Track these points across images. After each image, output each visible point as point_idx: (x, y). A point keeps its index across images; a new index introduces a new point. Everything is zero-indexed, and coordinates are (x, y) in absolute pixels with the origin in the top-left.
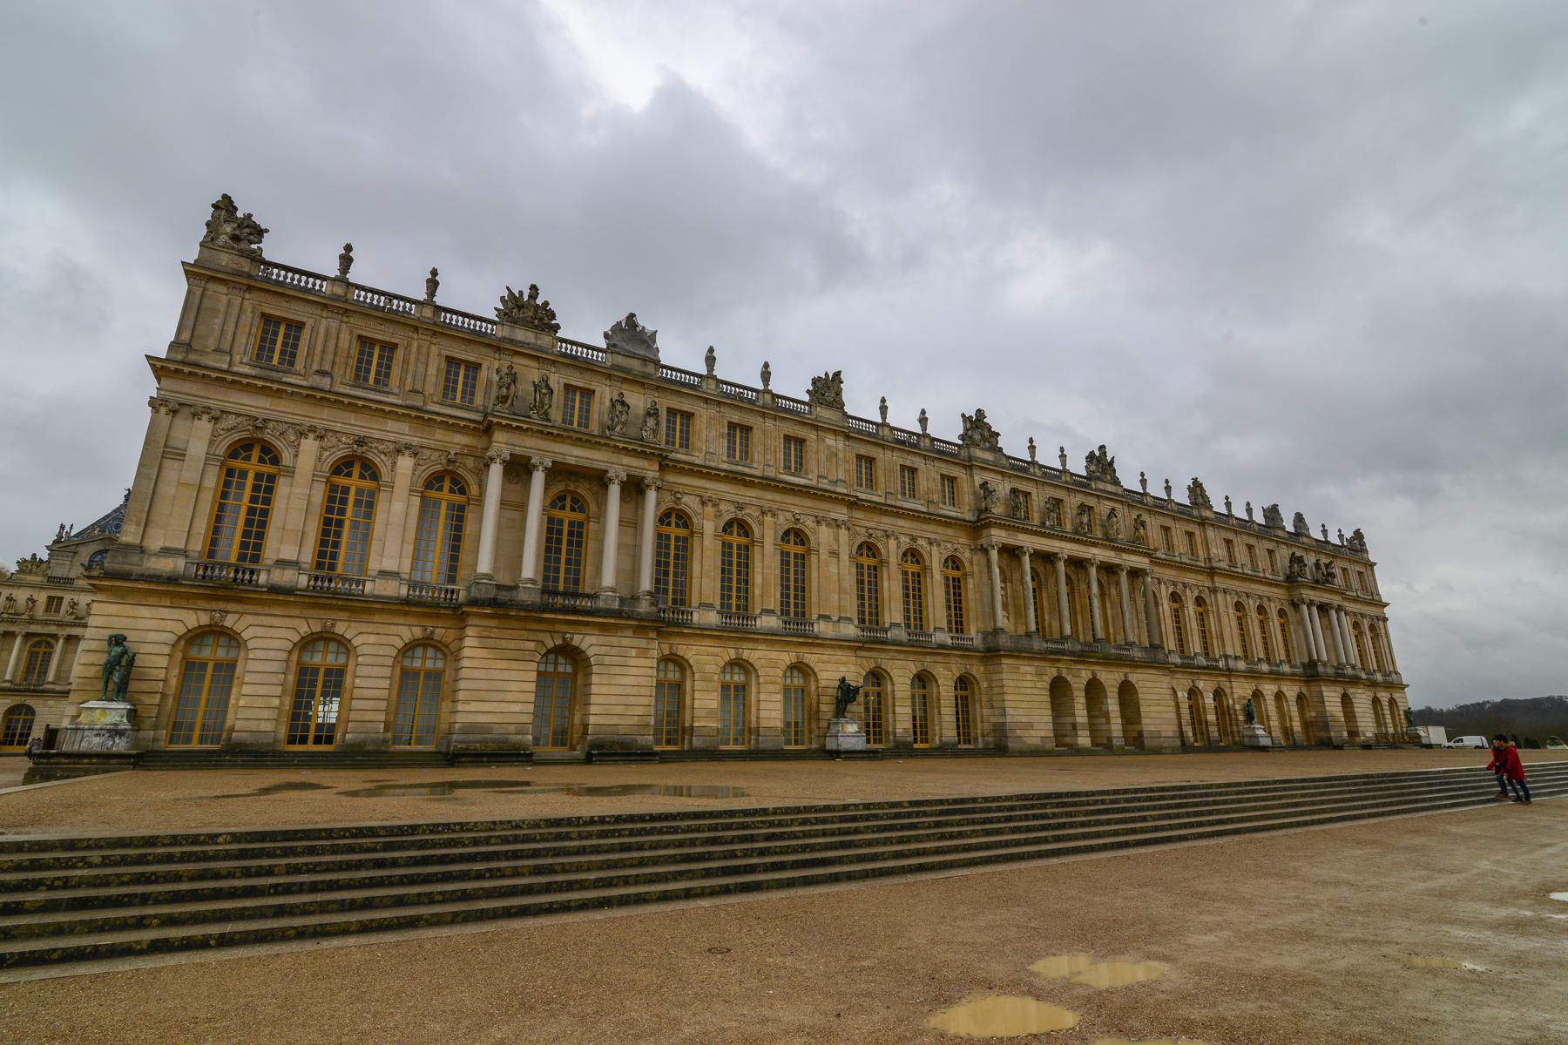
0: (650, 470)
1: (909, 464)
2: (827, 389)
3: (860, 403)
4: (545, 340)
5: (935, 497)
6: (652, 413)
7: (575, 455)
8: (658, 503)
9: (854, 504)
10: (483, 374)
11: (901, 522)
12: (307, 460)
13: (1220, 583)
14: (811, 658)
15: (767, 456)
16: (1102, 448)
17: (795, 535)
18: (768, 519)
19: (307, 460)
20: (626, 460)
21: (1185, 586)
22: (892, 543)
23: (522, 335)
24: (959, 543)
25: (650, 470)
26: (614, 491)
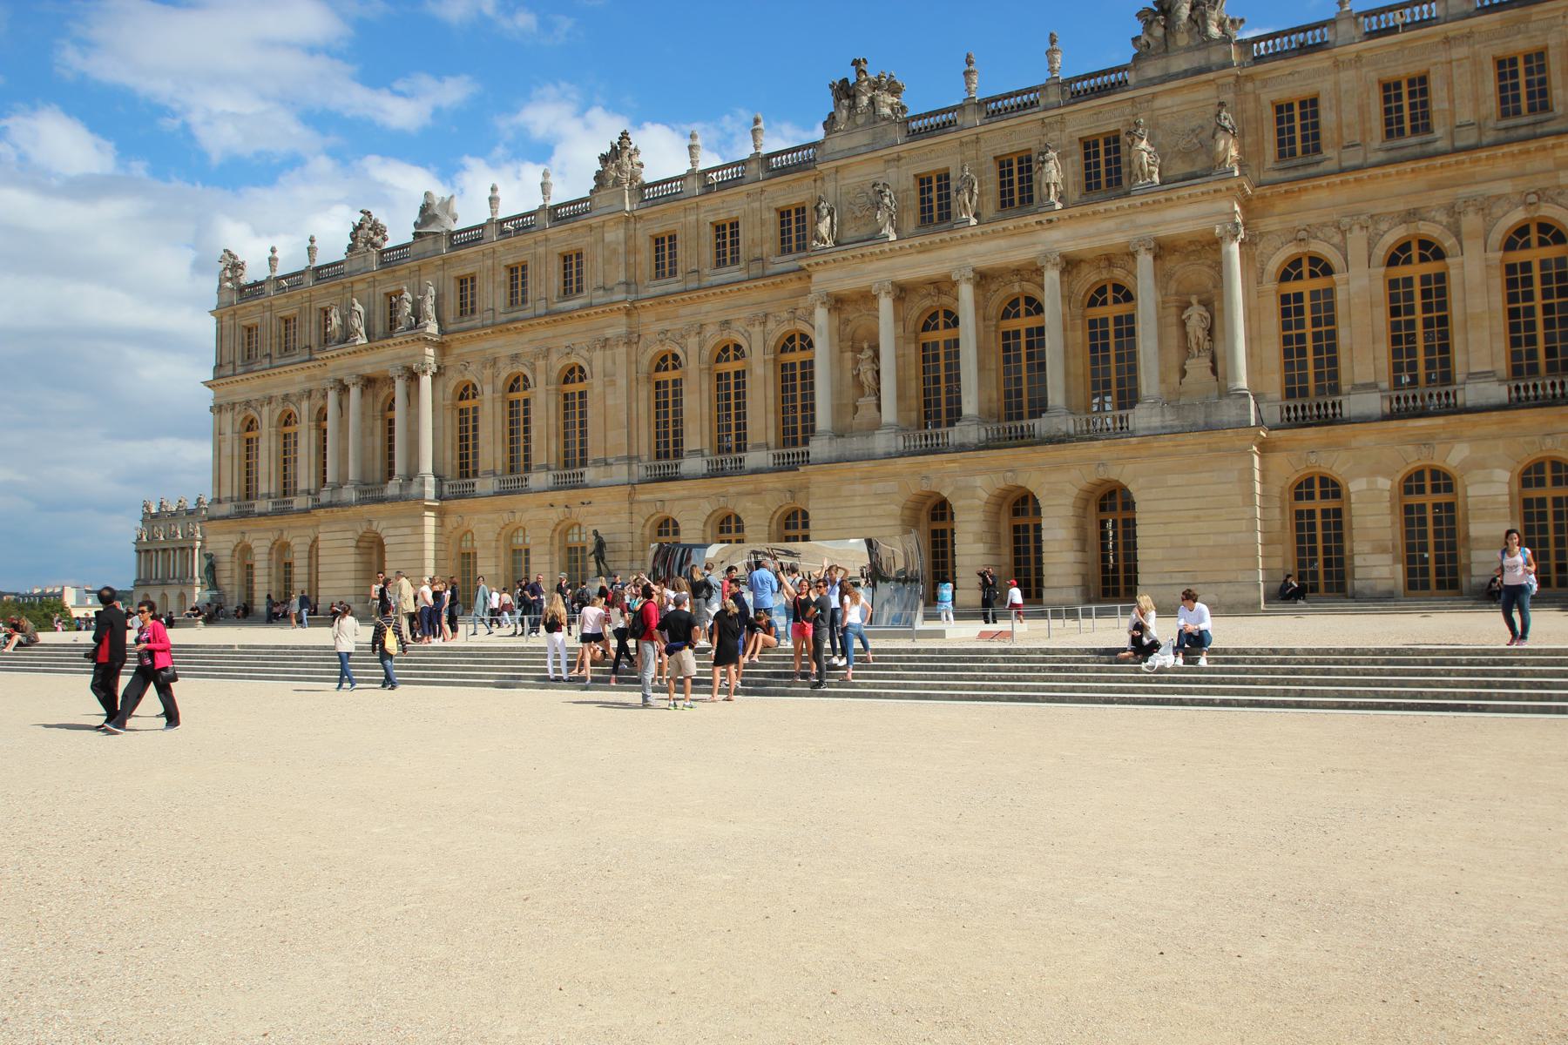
1: (722, 216)
5: (766, 248)
11: (706, 307)
12: (267, 420)
14: (579, 513)
17: (573, 374)
19: (267, 420)
22: (693, 342)
26: (400, 387)
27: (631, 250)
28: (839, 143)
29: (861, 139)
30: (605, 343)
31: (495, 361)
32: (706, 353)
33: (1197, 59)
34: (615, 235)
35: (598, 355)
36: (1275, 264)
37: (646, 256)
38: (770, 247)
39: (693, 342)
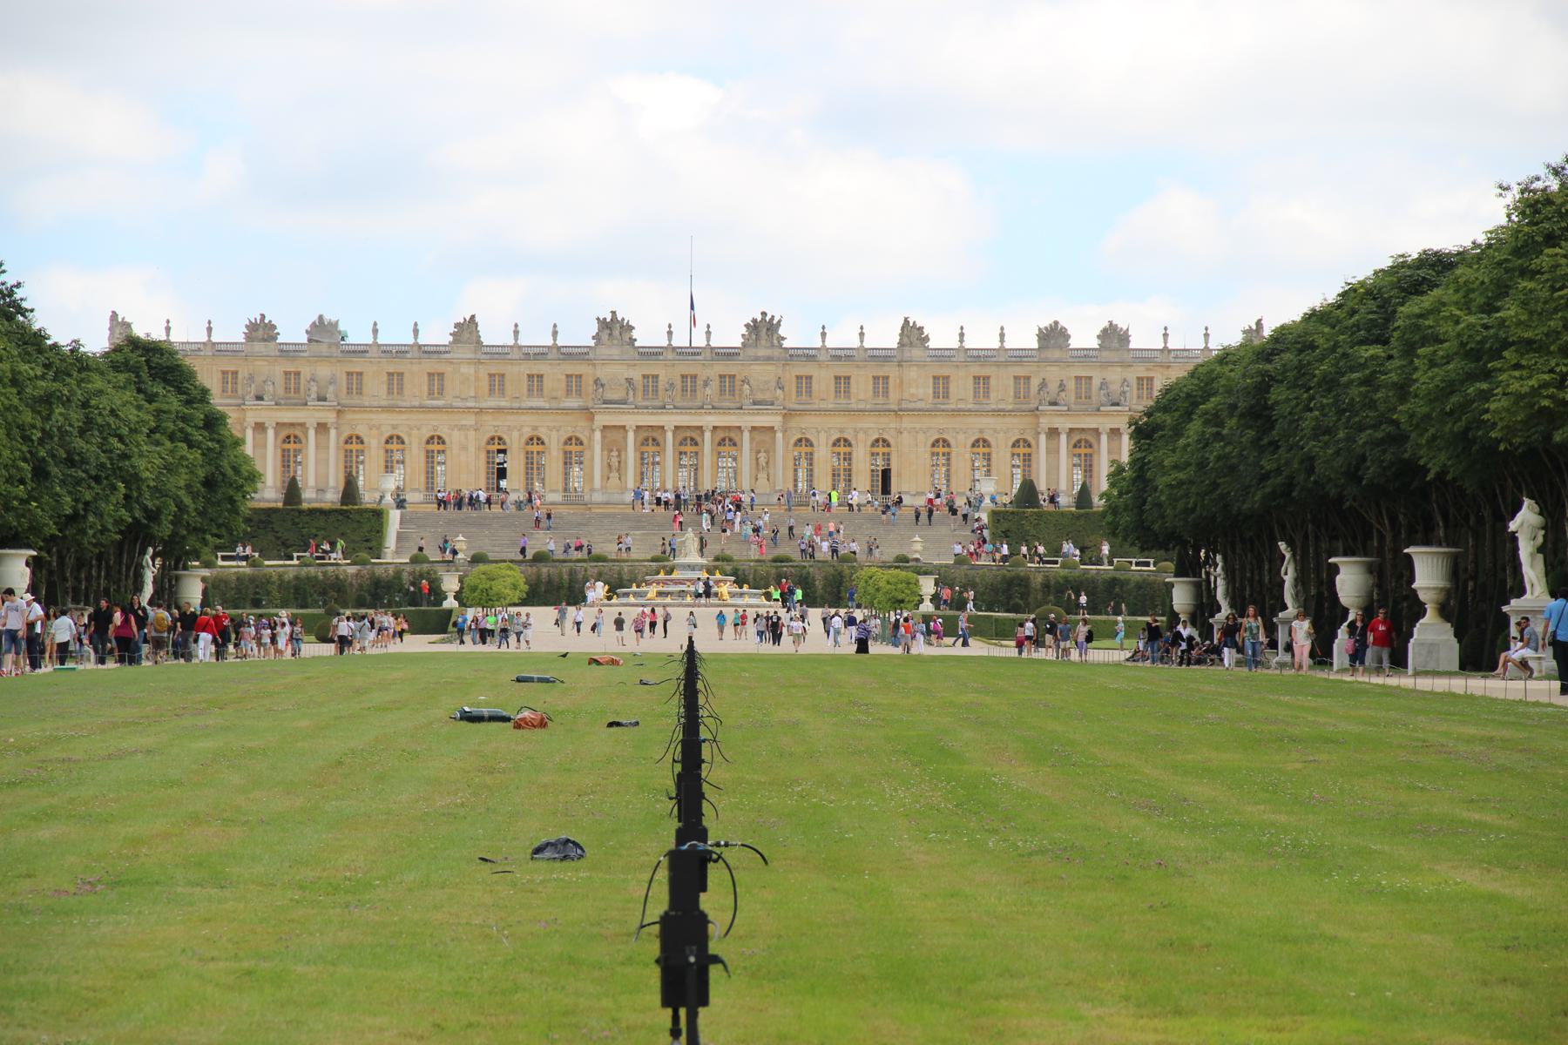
0: (330, 417)
2: (467, 329)
3: (493, 334)
4: (271, 345)
6: (332, 381)
7: (288, 416)
8: (338, 435)
9: (481, 411)
10: (240, 376)
11: (523, 418)
13: (907, 423)
15: (416, 388)
16: (764, 314)
18: (415, 432)
20: (317, 414)
21: (856, 431)
22: (515, 434)
23: (259, 347)
24: (579, 428)
25: (330, 417)
26: (312, 433)
27: (477, 379)
28: (603, 351)
29: (615, 352)
30: (462, 428)
31: (378, 428)
32: (523, 440)
33: (768, 352)
34: (467, 370)
35: (456, 433)
36: (792, 441)
37: (485, 383)
38: (560, 393)
39: (515, 434)
